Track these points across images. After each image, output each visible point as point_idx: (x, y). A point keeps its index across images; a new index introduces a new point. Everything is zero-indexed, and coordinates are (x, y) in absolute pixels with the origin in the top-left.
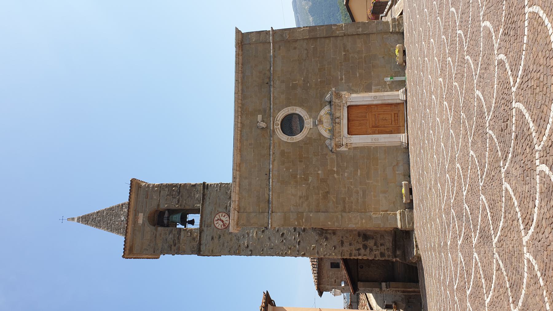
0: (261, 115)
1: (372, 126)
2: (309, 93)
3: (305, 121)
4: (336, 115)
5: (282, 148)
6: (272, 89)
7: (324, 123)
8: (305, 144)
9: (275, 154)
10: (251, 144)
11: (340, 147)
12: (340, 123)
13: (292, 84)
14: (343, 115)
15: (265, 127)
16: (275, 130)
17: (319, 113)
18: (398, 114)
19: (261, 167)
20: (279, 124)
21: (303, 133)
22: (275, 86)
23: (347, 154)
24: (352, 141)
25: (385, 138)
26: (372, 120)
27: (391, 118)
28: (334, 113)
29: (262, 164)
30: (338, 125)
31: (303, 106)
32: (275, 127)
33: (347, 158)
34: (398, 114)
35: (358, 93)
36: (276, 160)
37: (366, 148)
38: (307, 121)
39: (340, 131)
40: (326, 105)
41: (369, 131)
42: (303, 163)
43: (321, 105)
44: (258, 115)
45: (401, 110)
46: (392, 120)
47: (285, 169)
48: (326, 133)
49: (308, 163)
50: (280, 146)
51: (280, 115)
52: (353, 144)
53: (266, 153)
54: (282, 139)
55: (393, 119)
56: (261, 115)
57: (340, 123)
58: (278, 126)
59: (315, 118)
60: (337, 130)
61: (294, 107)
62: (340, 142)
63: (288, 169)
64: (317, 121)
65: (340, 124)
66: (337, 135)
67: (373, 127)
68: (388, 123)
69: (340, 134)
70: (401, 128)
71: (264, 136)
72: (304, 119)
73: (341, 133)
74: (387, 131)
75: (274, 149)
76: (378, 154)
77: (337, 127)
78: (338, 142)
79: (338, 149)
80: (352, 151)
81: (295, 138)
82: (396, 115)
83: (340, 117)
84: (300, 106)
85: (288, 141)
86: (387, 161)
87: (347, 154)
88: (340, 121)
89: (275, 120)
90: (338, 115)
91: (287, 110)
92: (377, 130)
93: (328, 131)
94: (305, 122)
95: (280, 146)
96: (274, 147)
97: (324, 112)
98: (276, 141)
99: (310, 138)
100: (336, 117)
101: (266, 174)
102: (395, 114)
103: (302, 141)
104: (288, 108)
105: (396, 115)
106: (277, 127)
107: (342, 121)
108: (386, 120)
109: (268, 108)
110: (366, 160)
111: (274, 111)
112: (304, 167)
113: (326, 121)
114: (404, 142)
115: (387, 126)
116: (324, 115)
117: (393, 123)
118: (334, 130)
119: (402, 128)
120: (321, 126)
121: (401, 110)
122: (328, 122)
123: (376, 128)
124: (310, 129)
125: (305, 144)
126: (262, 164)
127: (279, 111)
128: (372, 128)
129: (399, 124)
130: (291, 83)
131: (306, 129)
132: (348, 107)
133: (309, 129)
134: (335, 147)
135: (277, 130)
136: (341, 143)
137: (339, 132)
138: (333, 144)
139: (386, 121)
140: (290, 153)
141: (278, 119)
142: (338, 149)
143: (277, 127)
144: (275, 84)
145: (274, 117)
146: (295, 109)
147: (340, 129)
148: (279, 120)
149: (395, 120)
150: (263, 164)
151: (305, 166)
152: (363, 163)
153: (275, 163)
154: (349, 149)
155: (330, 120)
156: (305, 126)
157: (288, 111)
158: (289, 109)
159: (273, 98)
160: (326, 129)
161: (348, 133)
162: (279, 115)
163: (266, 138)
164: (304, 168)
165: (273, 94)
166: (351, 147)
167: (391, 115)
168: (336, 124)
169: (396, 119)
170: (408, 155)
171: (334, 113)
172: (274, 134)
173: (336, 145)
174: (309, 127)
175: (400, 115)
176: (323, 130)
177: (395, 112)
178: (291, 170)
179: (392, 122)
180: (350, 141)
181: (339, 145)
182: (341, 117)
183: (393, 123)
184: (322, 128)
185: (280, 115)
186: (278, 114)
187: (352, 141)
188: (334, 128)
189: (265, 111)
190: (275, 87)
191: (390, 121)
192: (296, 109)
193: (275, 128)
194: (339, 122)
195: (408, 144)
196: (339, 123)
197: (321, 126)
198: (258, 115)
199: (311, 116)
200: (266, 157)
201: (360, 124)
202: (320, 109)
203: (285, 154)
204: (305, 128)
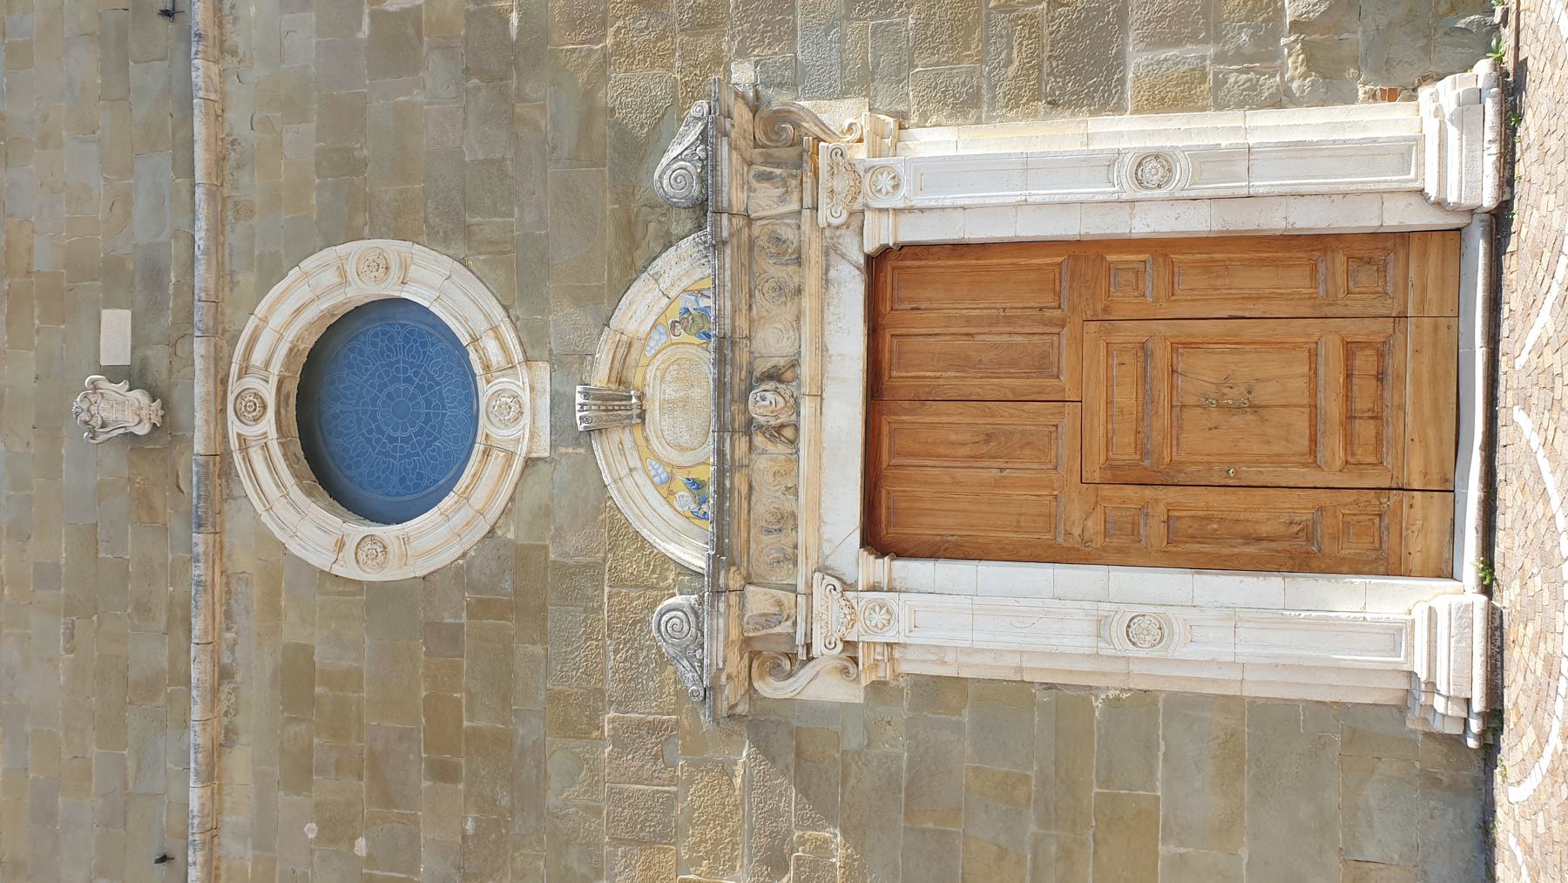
0: (127, 314)
1: (1111, 466)
2: (520, 109)
3: (481, 383)
4: (758, 345)
5: (292, 631)
6: (200, 70)
7: (653, 414)
8: (480, 609)
9: (238, 678)
10: (46, 575)
11: (787, 664)
12: (788, 432)
13: (373, 15)
14: (822, 349)
15: (142, 430)
16: (237, 458)
17: (607, 307)
18: (1381, 355)
19: (126, 785)
20: (265, 407)
21: (466, 497)
22: (235, 39)
23: (853, 740)
24: (904, 624)
25: (1234, 616)
26: (1109, 403)
27: (1314, 393)
28: (742, 322)
29: (131, 764)
30: (771, 448)
31: (467, 233)
32: (235, 428)
33: (852, 781)
34: (1381, 355)
35: (978, 121)
36: (243, 739)
37: (1044, 697)
38: (503, 382)
39: (788, 506)
40: (676, 229)
41: (1079, 519)
42: (461, 786)
43: (629, 231)
44: (106, 314)
45: (1422, 303)
46: (1314, 408)
47: (311, 830)
48: (665, 510)
49: (505, 801)
50: (272, 608)
51: (275, 321)
52: (910, 655)
53: (166, 666)
54: (294, 547)
55: (1332, 408)
56: (127, 314)
57: (797, 428)
58: (256, 420)
59: (571, 361)
60: (765, 503)
61: (394, 248)
62: (785, 628)
63: (337, 829)
64: (586, 395)
65: (793, 442)
66: (764, 547)
67: (1117, 476)
68: (1277, 448)
69: (786, 540)
70: (1418, 511)
71: (151, 508)
72: (478, 368)
73: (795, 528)
74: (1264, 530)
75: (229, 636)
76: (1151, 772)
77: (761, 463)
78: (767, 620)
79: (770, 688)
80: (903, 711)
81: (394, 548)
82: (1365, 362)
83: (794, 364)
84: (438, 238)
85: (338, 570)
86: (1244, 854)
87: (853, 740)
88: (797, 404)
89: (234, 369)
90: (772, 344)
91: (330, 277)
92: (1161, 508)
93: (684, 497)
94: (483, 401)
95: (272, 608)
96: (228, 615)
97: (657, 310)
98: (244, 560)
99: (524, 559)
100: (762, 367)
101: (164, 859)
102: (1350, 349)
103: (458, 574)
104: (342, 249)
105: (1365, 362)
106: (251, 431)
107: (807, 407)
108: (1255, 408)
109: (177, 250)
110: (1033, 828)
111: (224, 274)
112: (470, 826)
113: (671, 392)
114: (1442, 686)
115: (1268, 475)
116: (659, 339)
117: (1334, 449)
118: (737, 503)
119: (1421, 513)
120: (628, 444)
121: (1422, 303)
122: (686, 401)
123: (1148, 492)
124: (530, 462)
125: (480, 609)
126: (131, 764)
127: (271, 273)
128: (1107, 491)
129: (1388, 461)
130: (367, 10)
131: (497, 459)
132: (876, 263)
133: (518, 464)
134: (736, 663)
135: (247, 460)
136: (800, 639)
137: (785, 521)
138: (719, 651)
139: (1251, 417)
140: (360, 688)
141: (258, 358)
142: (770, 688)
143: (251, 431)
144: (236, 19)
145: (223, 336)
146: (394, 268)
147: (794, 491)
148: (267, 364)
149: (1350, 417)
150: (139, 769)
151: (477, 820)
152: (1002, 854)
153: (240, 764)
154: (877, 687)
155: (703, 392)
156: (480, 438)
157: (344, 281)
158: (350, 269)
159: (221, 160)
160: (671, 478)
161: (875, 540)
162: (265, 320)
163: (165, 527)
164: (464, 837)
165: (218, 117)
166: (896, 676)
167: (1313, 355)
168: (759, 440)
169: (1363, 403)
170: (1473, 818)
171: (742, 322)
172: (231, 497)
173: (750, 649)
174: (522, 450)
175: (1412, 364)
176: (639, 477)
177: (1358, 331)
178: (361, 847)
179: (1313, 440)
180: (879, 617)
181: (785, 648)
182: (806, 370)
183: (1334, 449)
184: (634, 461)
185: (275, 321)
186: (261, 310)
187: (904, 624)
188: (740, 482)
189: (154, 275)
190: (234, 53)
191: (1301, 422)
192: (404, 267)
193: (234, 443)
194: (783, 419)
195: (1494, 716)
196: (784, 432)
197: (628, 444)
198: (106, 314)
199: (533, 343)
200: (161, 701)
201: (989, 437)
202: (616, 272)
203: (318, 690)
204: (487, 453)
